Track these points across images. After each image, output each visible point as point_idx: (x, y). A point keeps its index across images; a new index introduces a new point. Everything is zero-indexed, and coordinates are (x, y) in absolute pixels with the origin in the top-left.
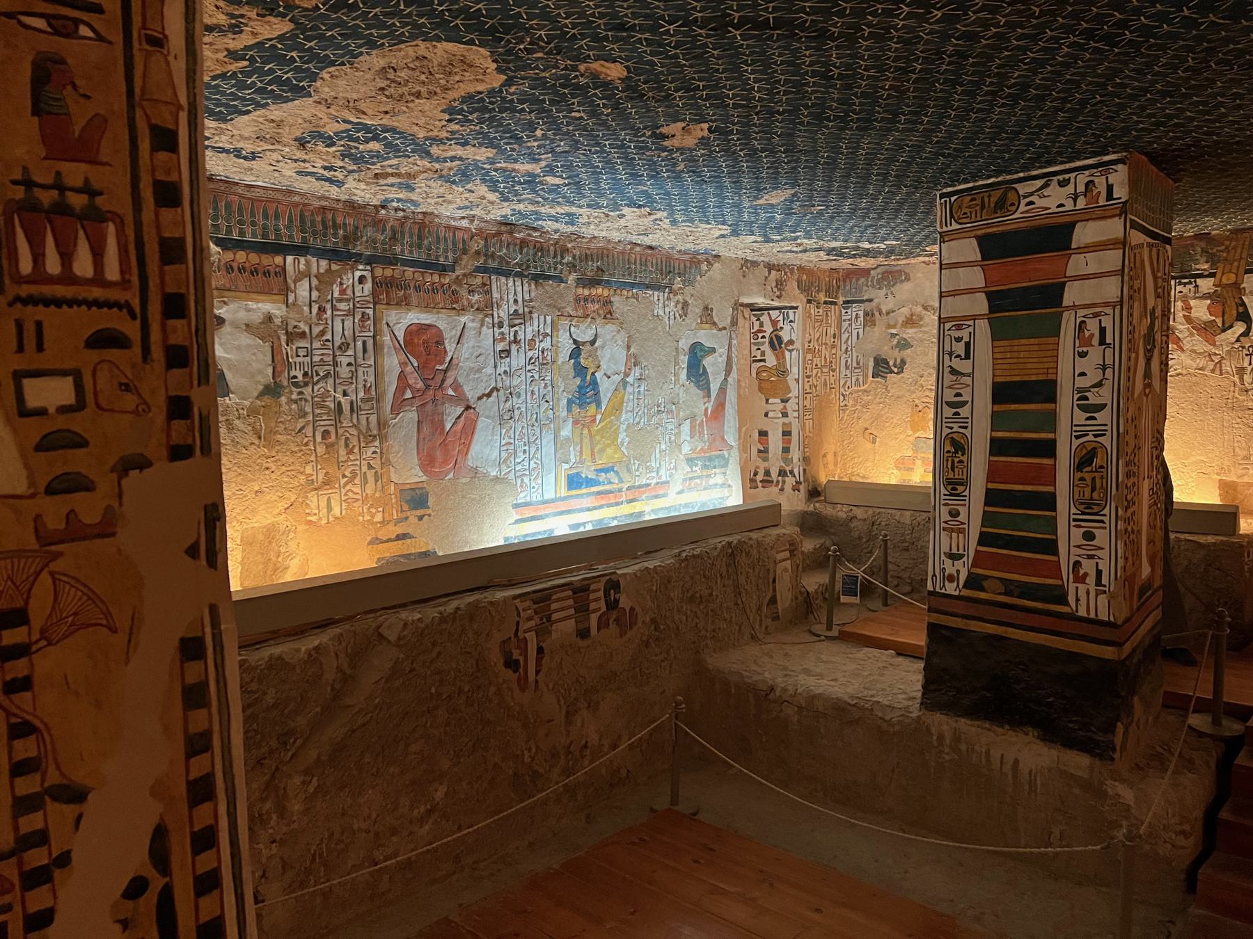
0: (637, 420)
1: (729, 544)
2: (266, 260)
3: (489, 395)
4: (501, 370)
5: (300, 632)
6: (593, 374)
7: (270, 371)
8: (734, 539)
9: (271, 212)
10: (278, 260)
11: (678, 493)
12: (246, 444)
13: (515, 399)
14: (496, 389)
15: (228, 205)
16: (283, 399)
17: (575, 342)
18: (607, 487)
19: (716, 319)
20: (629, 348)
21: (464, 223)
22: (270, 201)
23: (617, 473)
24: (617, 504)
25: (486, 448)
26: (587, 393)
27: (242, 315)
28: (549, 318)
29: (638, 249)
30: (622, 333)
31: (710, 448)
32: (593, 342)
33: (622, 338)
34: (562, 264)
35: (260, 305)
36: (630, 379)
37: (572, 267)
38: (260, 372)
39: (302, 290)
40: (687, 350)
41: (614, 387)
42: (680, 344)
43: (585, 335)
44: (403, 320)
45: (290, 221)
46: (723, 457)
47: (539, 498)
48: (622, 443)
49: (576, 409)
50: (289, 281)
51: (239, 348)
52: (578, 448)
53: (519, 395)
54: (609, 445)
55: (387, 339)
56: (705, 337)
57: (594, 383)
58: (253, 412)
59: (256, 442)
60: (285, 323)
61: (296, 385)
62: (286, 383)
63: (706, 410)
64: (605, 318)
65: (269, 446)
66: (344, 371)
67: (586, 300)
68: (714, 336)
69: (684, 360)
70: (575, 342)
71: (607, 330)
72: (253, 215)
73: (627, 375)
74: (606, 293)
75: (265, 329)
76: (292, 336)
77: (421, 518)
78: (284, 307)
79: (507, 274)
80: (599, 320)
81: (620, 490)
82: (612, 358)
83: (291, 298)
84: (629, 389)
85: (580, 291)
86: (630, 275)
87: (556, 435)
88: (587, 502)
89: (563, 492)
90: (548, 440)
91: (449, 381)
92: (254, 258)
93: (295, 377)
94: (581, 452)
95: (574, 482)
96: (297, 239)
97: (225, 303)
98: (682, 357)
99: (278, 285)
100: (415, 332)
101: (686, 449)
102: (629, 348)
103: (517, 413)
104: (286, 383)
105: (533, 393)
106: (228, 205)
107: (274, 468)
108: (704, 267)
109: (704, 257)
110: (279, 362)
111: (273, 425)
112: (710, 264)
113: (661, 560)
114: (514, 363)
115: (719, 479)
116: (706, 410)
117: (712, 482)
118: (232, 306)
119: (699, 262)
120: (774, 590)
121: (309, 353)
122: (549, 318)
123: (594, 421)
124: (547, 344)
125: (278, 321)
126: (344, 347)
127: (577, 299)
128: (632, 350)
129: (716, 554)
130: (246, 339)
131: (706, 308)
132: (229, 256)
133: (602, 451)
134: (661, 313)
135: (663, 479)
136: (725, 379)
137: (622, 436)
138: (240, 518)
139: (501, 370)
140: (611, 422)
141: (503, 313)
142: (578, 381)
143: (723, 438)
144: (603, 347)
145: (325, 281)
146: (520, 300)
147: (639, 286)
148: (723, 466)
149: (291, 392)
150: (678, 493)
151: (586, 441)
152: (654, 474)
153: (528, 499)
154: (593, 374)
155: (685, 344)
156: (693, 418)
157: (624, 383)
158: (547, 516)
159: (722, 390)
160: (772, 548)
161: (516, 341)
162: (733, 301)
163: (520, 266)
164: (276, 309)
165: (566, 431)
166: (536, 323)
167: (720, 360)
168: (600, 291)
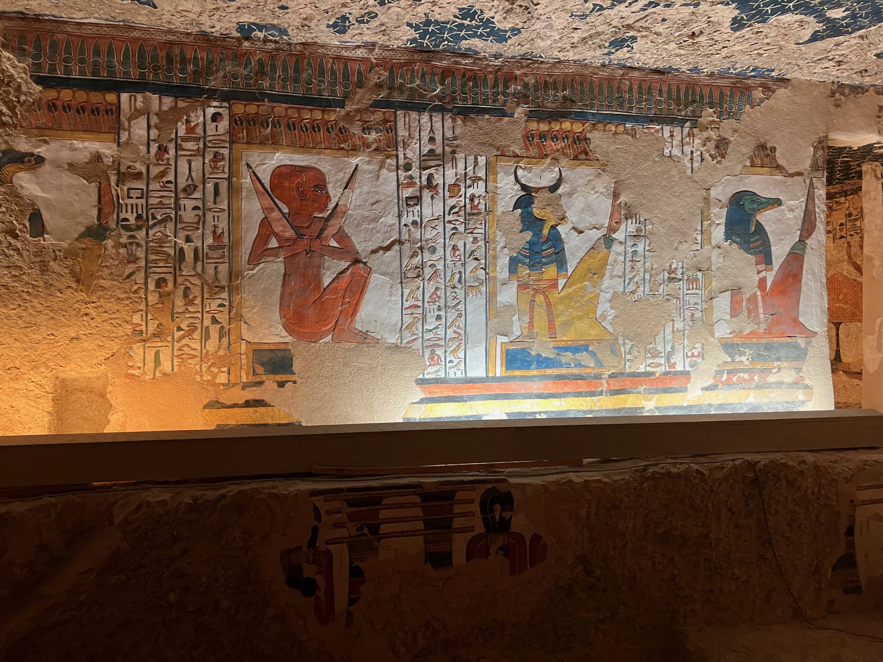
0: (631, 287)
1: (752, 465)
2: (95, 98)
3: (388, 248)
4: (407, 219)
5: (23, 494)
6: (553, 227)
7: (94, 212)
8: (763, 459)
9: (104, 48)
10: (111, 97)
11: (707, 389)
12: (62, 287)
13: (427, 255)
14: (400, 242)
15: (54, 45)
16: (109, 243)
17: (524, 187)
18: (575, 371)
19: (781, 162)
20: (616, 195)
21: (360, 53)
22: (103, 37)
23: (593, 354)
24: (593, 394)
25: (381, 307)
26: (542, 248)
27: (66, 155)
28: (482, 160)
29: (636, 74)
30: (605, 177)
31: (768, 332)
32: (553, 188)
33: (604, 184)
34: (504, 94)
35: (86, 144)
36: (619, 235)
37: (522, 98)
38: (83, 212)
39: (139, 129)
40: (725, 199)
41: (590, 245)
42: (713, 193)
43: (540, 176)
44: (269, 161)
45: (126, 56)
46: (796, 347)
47: (459, 375)
48: (604, 316)
49: (524, 271)
50: (122, 118)
51: (59, 188)
52: (527, 318)
53: (433, 250)
54: (580, 318)
55: (247, 181)
56: (760, 184)
57: (556, 240)
58: (70, 254)
59: (74, 285)
60: (117, 163)
61: (127, 228)
62: (113, 225)
63: (763, 281)
64: (576, 158)
65: (88, 289)
66: (189, 216)
67: (543, 136)
68: (777, 183)
69: (719, 215)
70: (524, 187)
71: (578, 175)
72: (82, 52)
73: (612, 229)
74: (578, 128)
75: (92, 169)
76: (122, 178)
77: (281, 384)
78: (115, 146)
79: (420, 108)
80: (564, 162)
81: (598, 377)
82: (588, 208)
83: (124, 136)
84: (617, 248)
85: (533, 126)
86: (621, 105)
87: (491, 298)
88: (537, 387)
89: (499, 371)
90: (476, 306)
91: (331, 230)
92: (82, 96)
93: (126, 220)
94: (531, 324)
95: (515, 359)
96: (134, 74)
97: (46, 142)
98: (715, 210)
99: (110, 122)
100: (281, 174)
101: (722, 331)
102: (616, 195)
103: (428, 272)
104: (113, 225)
105: (455, 248)
106: (54, 45)
107: (94, 314)
108: (758, 94)
109: (758, 81)
110: (106, 203)
111: (95, 268)
112: (766, 88)
113: (621, 472)
114: (427, 212)
115: (788, 376)
116: (763, 281)
117: (771, 379)
118: (54, 145)
119: (749, 88)
120: (851, 545)
121: (145, 195)
122: (482, 160)
123: (555, 286)
124: (479, 189)
125: (108, 161)
126: (189, 190)
127: (528, 137)
128: (622, 199)
129: (719, 475)
130: (68, 179)
131: (763, 147)
132: (52, 94)
133: (567, 324)
134: (676, 152)
135: (679, 368)
136: (802, 241)
137: (603, 306)
138: (51, 364)
139: (407, 219)
140: (584, 288)
141: (413, 153)
142: (528, 236)
143: (796, 321)
144: (570, 194)
145: (168, 119)
146: (439, 138)
147: (635, 119)
148: (795, 359)
149: (120, 236)
150: (707, 389)
151: (540, 311)
152: (662, 361)
153: (442, 375)
154: (553, 227)
155: (722, 192)
156: (736, 291)
157: (608, 240)
158: (472, 398)
159: (796, 257)
160: (848, 481)
161: (430, 185)
162: (815, 138)
163: (439, 97)
164: (106, 149)
165: (508, 295)
166: (461, 165)
167: (790, 215)
168: (567, 125)
